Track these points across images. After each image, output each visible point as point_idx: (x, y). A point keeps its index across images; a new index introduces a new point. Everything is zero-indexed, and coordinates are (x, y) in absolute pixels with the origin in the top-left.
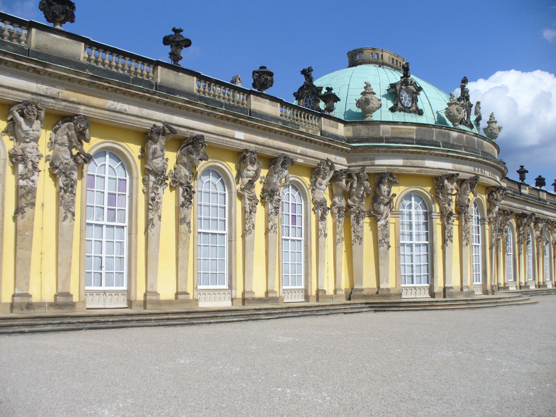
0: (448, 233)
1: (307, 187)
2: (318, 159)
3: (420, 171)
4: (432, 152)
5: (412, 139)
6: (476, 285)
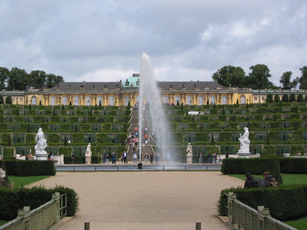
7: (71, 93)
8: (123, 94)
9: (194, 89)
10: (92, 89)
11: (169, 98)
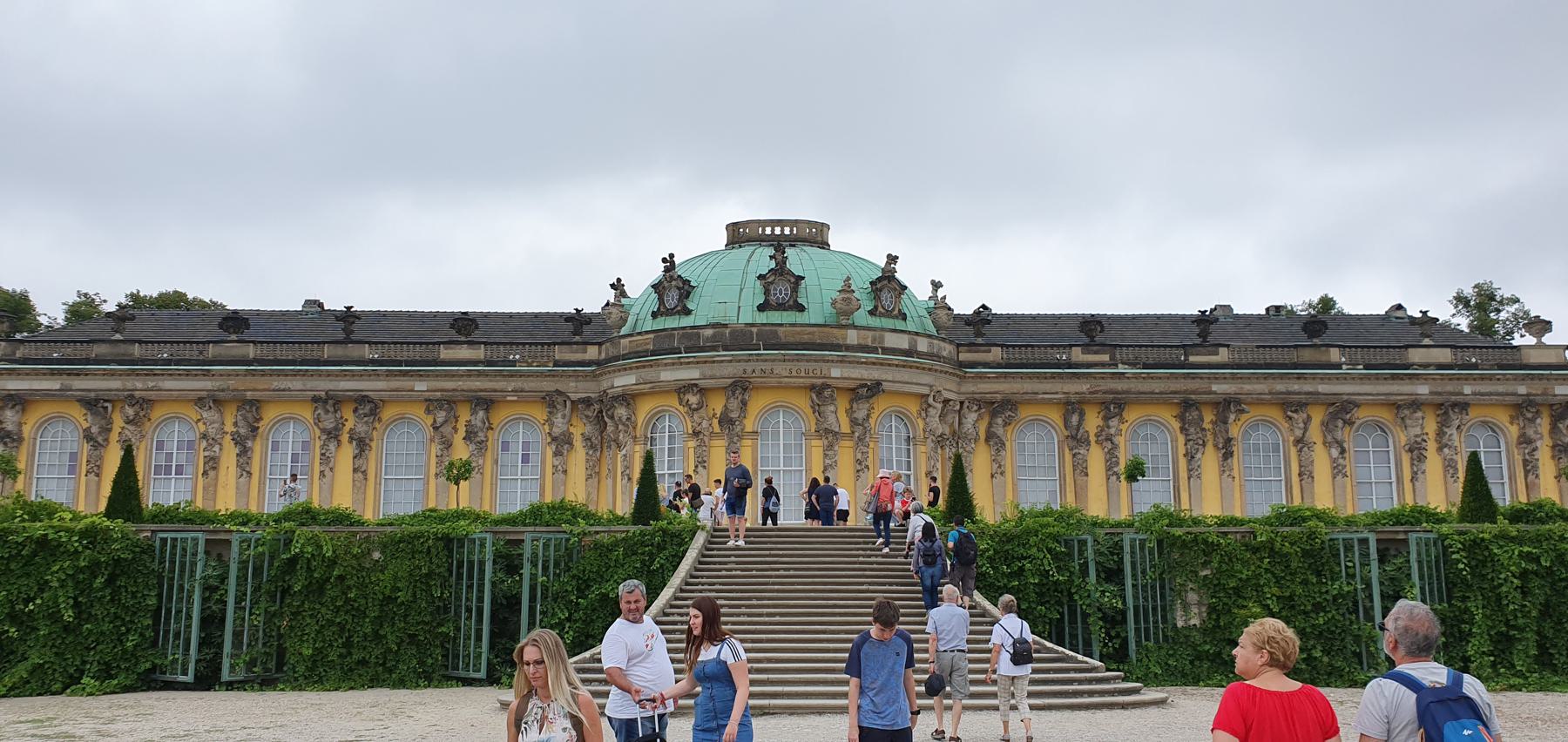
7: (115, 384)
8: (628, 398)
9: (1307, 355)
10: (327, 352)
11: (1076, 439)
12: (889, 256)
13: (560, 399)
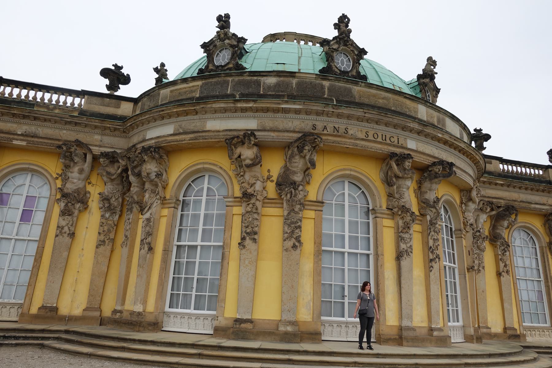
0: (247, 227)
1: (51, 176)
2: (59, 140)
3: (196, 139)
4: (209, 106)
5: (191, 99)
6: (454, 327)
8: (162, 152)
12: (430, 59)
13: (80, 151)
